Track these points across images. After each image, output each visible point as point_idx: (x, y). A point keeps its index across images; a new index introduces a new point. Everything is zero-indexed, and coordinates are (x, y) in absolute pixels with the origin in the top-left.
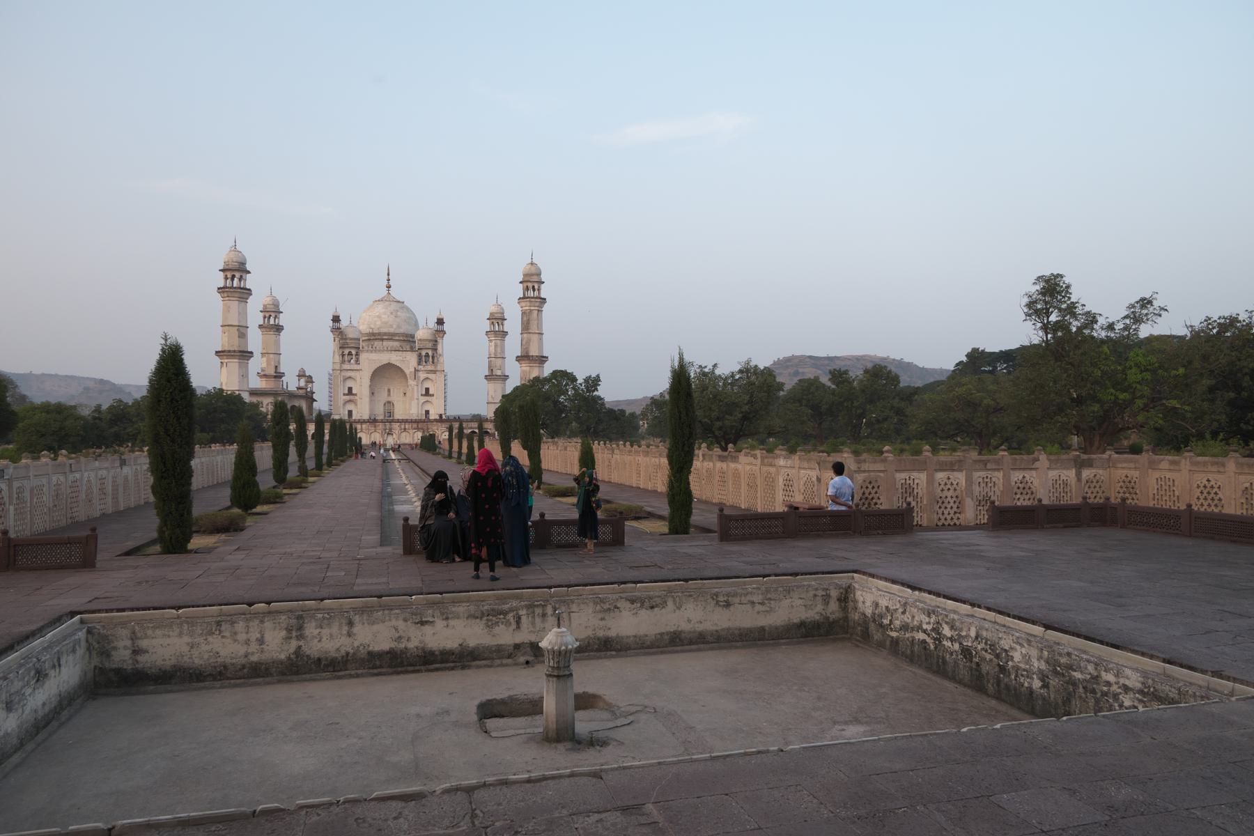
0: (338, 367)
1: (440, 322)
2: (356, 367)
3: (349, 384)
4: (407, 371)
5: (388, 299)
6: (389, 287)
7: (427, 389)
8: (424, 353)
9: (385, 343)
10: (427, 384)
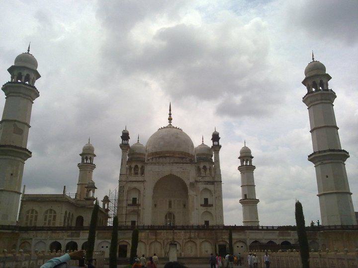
0: (124, 179)
1: (216, 137)
2: (140, 178)
4: (187, 183)
5: (170, 126)
6: (170, 119)
7: (206, 200)
8: (202, 166)
9: (168, 159)
10: (207, 196)
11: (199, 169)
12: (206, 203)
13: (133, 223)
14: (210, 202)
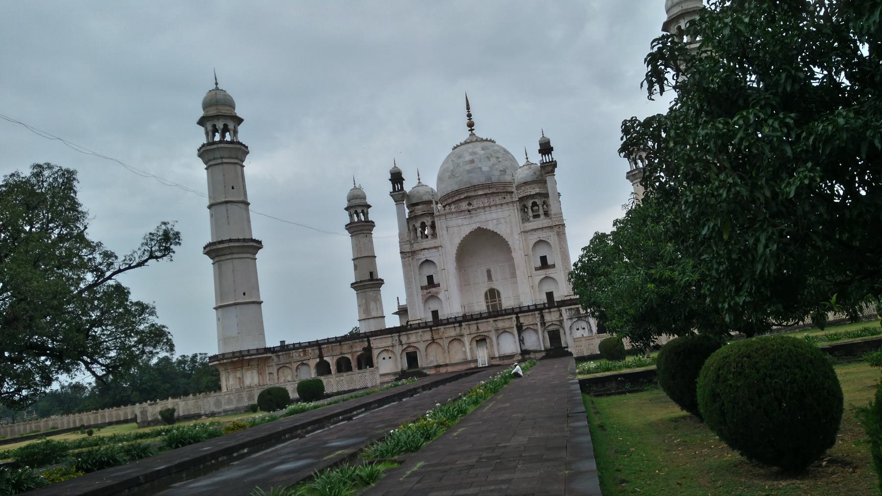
0: (407, 248)
1: (546, 148)
3: (428, 271)
7: (544, 259)
8: (529, 203)
11: (524, 209)
12: (544, 264)
13: (435, 313)
14: (550, 262)
